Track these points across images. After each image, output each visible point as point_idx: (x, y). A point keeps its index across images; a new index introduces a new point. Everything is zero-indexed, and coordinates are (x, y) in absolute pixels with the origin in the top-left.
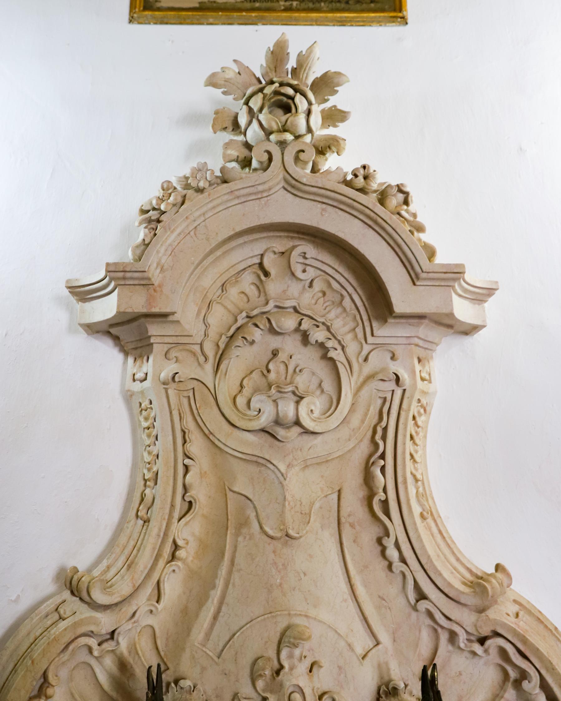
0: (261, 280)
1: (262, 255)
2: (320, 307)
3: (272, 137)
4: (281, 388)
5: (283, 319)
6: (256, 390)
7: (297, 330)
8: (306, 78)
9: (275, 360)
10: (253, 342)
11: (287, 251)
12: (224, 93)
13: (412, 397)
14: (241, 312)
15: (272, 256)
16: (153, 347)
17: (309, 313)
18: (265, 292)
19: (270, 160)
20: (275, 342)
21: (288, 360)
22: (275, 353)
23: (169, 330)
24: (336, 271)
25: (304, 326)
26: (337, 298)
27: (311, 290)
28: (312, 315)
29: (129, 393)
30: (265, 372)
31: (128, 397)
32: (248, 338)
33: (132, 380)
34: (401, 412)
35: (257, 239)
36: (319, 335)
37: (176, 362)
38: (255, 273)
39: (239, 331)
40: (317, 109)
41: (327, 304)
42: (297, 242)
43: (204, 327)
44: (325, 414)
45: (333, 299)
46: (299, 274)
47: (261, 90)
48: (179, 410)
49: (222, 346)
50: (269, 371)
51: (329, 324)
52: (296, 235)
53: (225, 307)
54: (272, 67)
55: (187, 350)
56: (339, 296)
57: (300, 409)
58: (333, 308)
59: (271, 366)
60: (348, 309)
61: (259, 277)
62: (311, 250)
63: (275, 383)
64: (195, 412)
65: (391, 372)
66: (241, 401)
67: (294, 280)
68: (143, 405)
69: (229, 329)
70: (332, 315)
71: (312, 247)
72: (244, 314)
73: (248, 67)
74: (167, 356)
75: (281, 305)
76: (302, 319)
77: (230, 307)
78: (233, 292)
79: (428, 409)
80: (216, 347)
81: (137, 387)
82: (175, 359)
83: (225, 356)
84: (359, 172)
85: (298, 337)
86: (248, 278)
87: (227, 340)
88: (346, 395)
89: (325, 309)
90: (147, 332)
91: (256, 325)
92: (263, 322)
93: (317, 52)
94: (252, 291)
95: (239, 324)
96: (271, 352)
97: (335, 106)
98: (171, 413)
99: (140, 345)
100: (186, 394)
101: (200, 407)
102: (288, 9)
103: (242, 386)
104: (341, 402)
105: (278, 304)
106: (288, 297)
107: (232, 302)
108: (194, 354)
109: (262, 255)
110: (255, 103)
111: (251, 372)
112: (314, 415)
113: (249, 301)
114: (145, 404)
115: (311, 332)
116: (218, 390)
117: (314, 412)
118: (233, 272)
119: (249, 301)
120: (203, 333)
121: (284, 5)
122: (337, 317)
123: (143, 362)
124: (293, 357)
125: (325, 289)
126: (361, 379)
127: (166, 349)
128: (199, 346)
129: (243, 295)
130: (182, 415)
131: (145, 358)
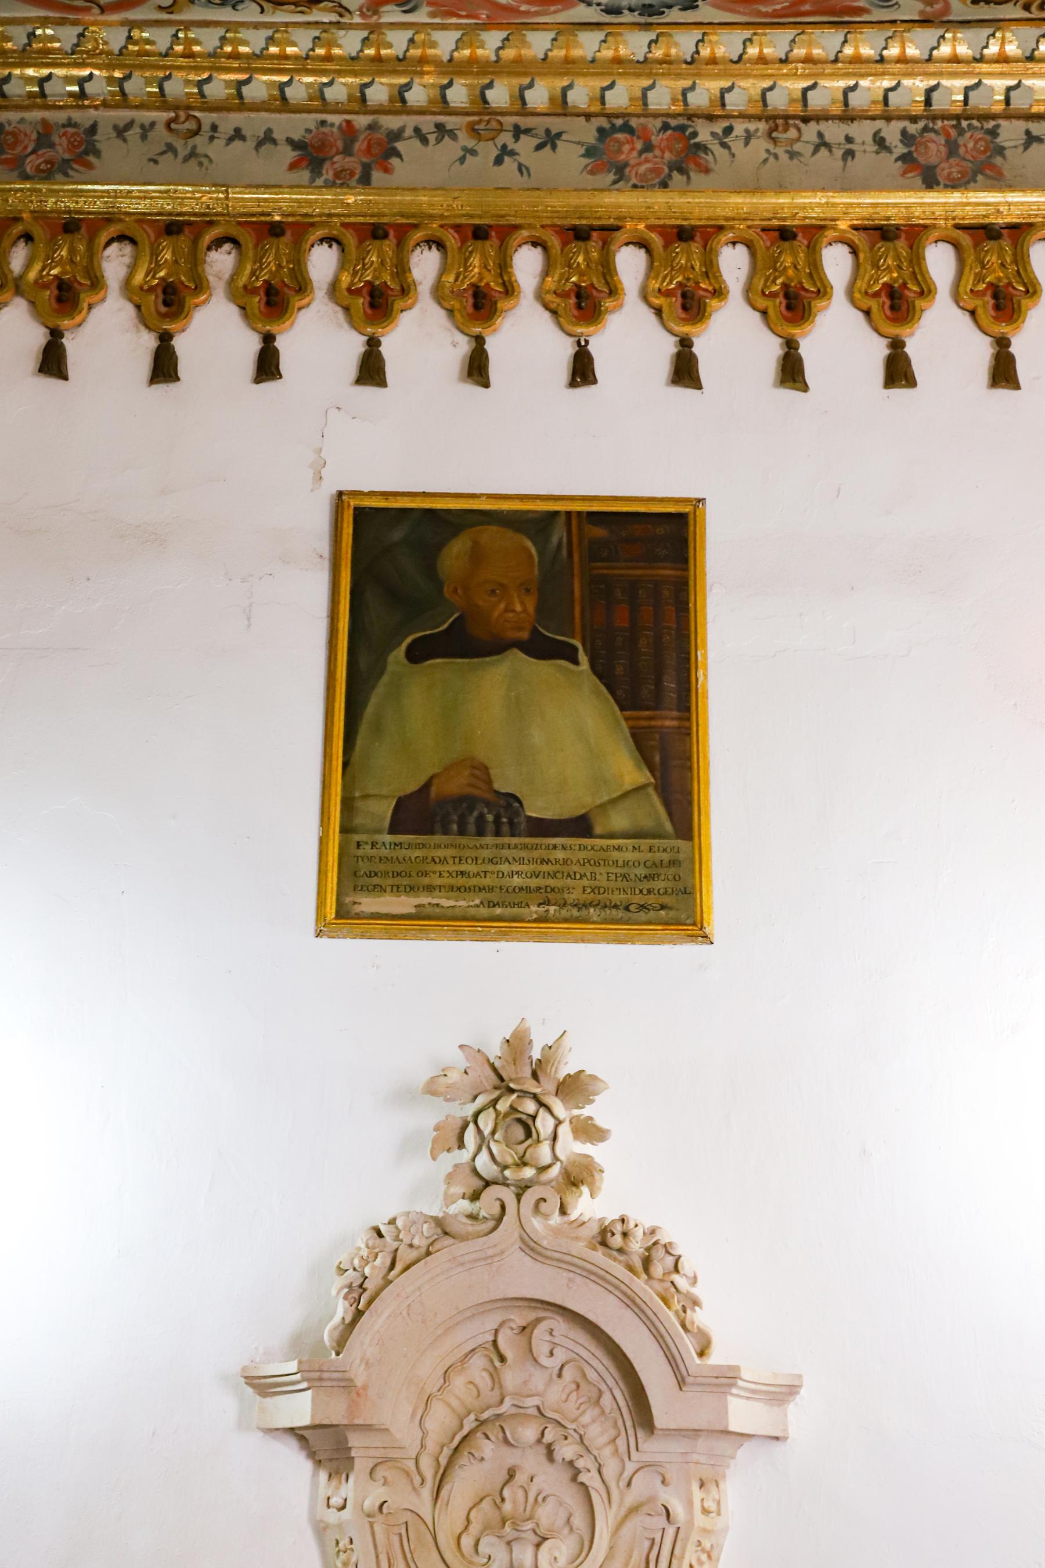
0: (495, 1367)
1: (497, 1331)
2: (571, 1407)
3: (507, 1173)
4: (518, 1525)
5: (520, 1429)
6: (486, 1528)
7: (539, 1441)
8: (556, 1072)
9: (511, 1484)
10: (482, 1459)
11: (528, 1324)
12: (447, 1100)
13: (687, 1539)
14: (469, 1413)
15: (508, 1332)
16: (353, 1462)
17: (555, 1416)
18: (500, 1383)
19: (503, 1208)
20: (512, 1458)
21: (528, 1485)
22: (511, 1474)
23: (374, 1440)
24: (593, 1354)
25: (548, 1437)
26: (594, 1394)
27: (560, 1381)
28: (559, 1420)
29: (322, 1525)
30: (498, 1501)
31: (320, 1529)
32: (476, 1455)
33: (325, 1505)
34: (673, 1560)
35: (490, 1310)
36: (566, 1451)
37: (384, 1485)
38: (486, 1356)
39: (465, 1443)
40: (564, 1131)
41: (581, 1400)
42: (542, 1314)
43: (420, 1434)
44: (573, 1562)
45: (589, 1394)
46: (544, 1360)
47: (494, 1103)
48: (388, 1554)
49: (443, 1461)
50: (503, 1500)
51: (582, 1433)
52: (539, 1305)
53: (449, 1405)
54: (510, 1059)
55: (398, 1468)
56: (596, 1390)
57: (540, 1557)
58: (588, 1408)
59: (506, 1493)
60: (607, 1411)
61: (492, 1361)
62: (559, 1325)
63: (510, 1517)
64: (409, 1556)
65: (660, 1505)
66: (467, 1542)
67: (538, 1367)
68: (341, 1545)
69: (453, 1438)
70: (586, 1419)
71: (561, 1321)
72: (472, 1417)
73: (479, 1051)
74: (373, 1475)
75: (521, 1405)
76: (546, 1428)
77: (455, 1403)
78: (458, 1382)
79: (714, 1554)
80: (435, 1463)
81: (332, 1517)
82: (383, 1480)
83: (447, 1479)
84: (615, 1228)
85: (542, 1450)
86: (478, 1368)
87: (450, 1452)
88: (601, 1536)
89: (578, 1409)
90: (347, 1443)
91: (487, 1437)
92: (495, 1432)
93: (567, 1041)
94: (483, 1380)
95: (465, 1432)
96: (506, 1472)
97: (591, 1118)
98: (377, 1557)
99: (336, 1456)
100: (396, 1530)
101: (415, 1549)
102: (542, 919)
103: (468, 1520)
104: (594, 1546)
105: (515, 1403)
106: (530, 1392)
107: (458, 1398)
108: (408, 1474)
109: (497, 1331)
110: (487, 1122)
111: (481, 1500)
112: (559, 1564)
113: (479, 1396)
114: (344, 1543)
115: (556, 1447)
116: (438, 1521)
117: (558, 1560)
118: (459, 1354)
119: (479, 1396)
120: (419, 1443)
121: (536, 912)
122: (594, 1421)
123: (340, 1483)
124: (534, 1480)
125: (579, 1380)
126: (623, 1511)
127: (371, 1465)
128: (414, 1461)
129: (471, 1386)
130: (392, 1561)
131: (344, 1476)
